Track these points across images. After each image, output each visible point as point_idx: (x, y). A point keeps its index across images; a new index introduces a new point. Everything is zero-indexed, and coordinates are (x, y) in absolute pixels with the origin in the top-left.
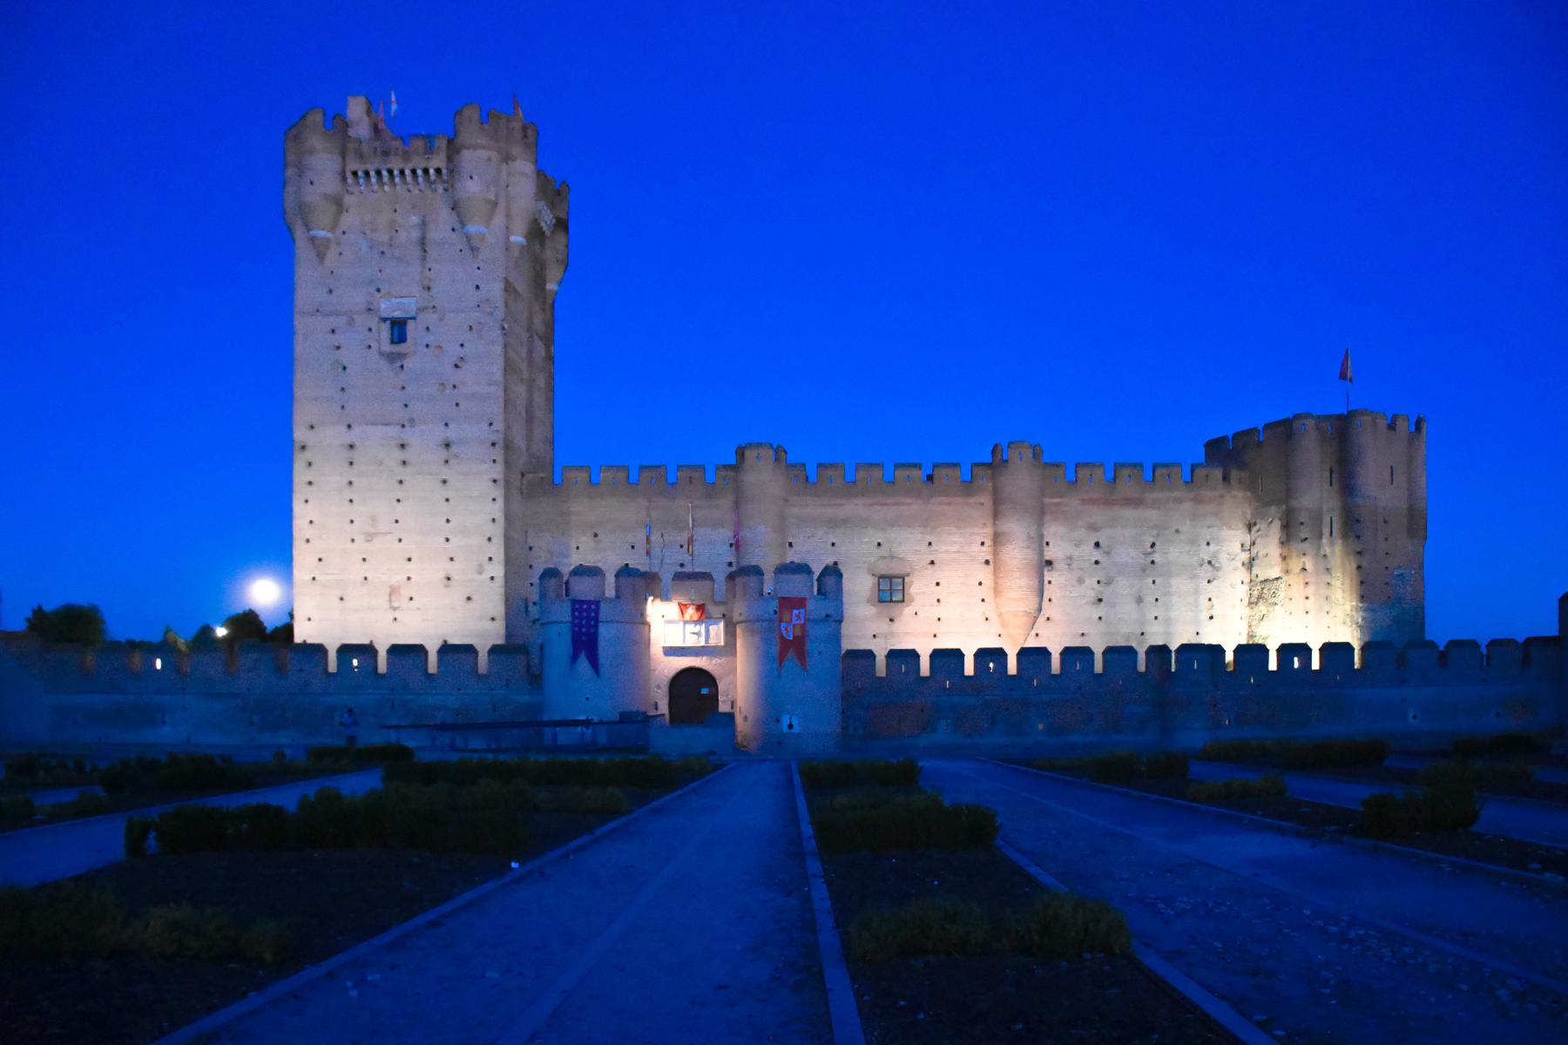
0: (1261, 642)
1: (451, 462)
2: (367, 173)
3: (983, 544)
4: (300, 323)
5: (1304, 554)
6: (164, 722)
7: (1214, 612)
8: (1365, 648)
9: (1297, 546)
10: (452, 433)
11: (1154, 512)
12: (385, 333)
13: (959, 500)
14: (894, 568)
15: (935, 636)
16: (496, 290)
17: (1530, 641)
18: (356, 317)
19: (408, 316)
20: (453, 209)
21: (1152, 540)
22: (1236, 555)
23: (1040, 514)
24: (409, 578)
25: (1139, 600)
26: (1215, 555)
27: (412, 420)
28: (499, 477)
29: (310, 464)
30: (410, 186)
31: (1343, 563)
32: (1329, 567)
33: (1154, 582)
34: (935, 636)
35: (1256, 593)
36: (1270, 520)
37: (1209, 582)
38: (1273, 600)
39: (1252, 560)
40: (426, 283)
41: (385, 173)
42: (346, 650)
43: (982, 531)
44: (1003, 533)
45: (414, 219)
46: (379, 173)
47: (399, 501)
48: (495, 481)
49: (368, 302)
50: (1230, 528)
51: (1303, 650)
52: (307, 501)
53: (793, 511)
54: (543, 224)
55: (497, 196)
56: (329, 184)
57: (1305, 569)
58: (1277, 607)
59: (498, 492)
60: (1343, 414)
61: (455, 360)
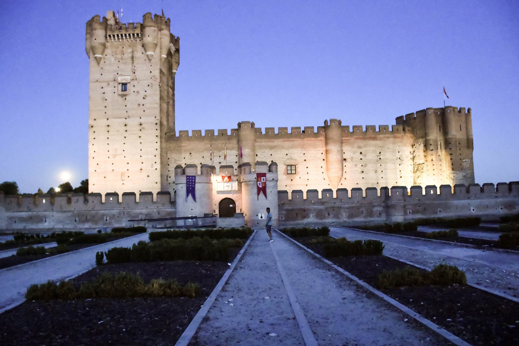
0: (418, 185)
1: (142, 130)
2: (114, 36)
3: (322, 153)
4: (92, 85)
5: (432, 155)
6: (46, 221)
7: (401, 175)
8: (455, 186)
9: (429, 152)
10: (142, 121)
11: (380, 142)
12: (120, 87)
13: (313, 139)
14: (292, 162)
15: (307, 185)
16: (157, 73)
17: (511, 184)
18: (110, 83)
20: (142, 46)
21: (380, 151)
22: (408, 156)
23: (342, 143)
25: (376, 172)
26: (401, 156)
27: (129, 116)
28: (159, 134)
29: (94, 132)
30: (128, 40)
31: (446, 158)
32: (440, 159)
33: (381, 165)
34: (307, 185)
35: (416, 169)
36: (420, 143)
37: (400, 165)
38: (422, 171)
39: (414, 157)
40: (134, 71)
41: (120, 35)
42: (108, 195)
43: (322, 149)
44: (329, 150)
45: (130, 50)
46: (118, 35)
47: (124, 143)
48: (157, 136)
49: (114, 78)
50: (405, 146)
51: (434, 187)
52: (93, 145)
53: (257, 144)
54: (172, 51)
55: (157, 42)
56: (102, 40)
57: (433, 160)
58: (423, 173)
59: (158, 140)
60: (443, 108)
61: (143, 96)
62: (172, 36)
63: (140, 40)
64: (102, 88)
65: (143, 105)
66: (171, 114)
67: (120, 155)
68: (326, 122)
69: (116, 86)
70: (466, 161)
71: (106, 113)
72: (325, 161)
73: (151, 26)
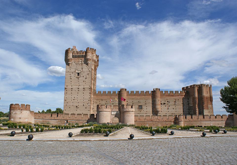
10: (84, 87)
12: (77, 74)
62: (96, 55)
66: (95, 84)
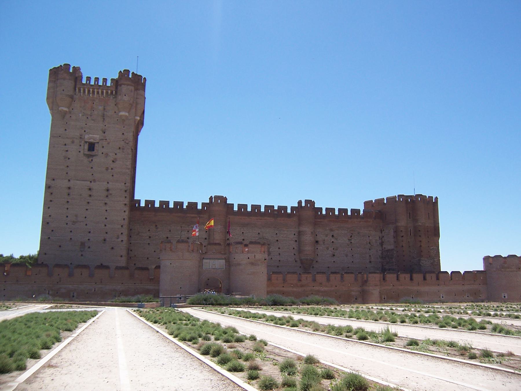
1: (109, 196)
10: (110, 186)
12: (86, 147)
19: (96, 142)
24: (89, 239)
28: (128, 203)
45: (101, 108)
47: (87, 210)
52: (49, 208)
63: (114, 98)
64: (65, 145)
65: (112, 169)
67: (81, 222)
68: (300, 202)
69: (82, 145)
70: (433, 249)
71: (67, 173)
72: (297, 243)
73: (128, 85)
